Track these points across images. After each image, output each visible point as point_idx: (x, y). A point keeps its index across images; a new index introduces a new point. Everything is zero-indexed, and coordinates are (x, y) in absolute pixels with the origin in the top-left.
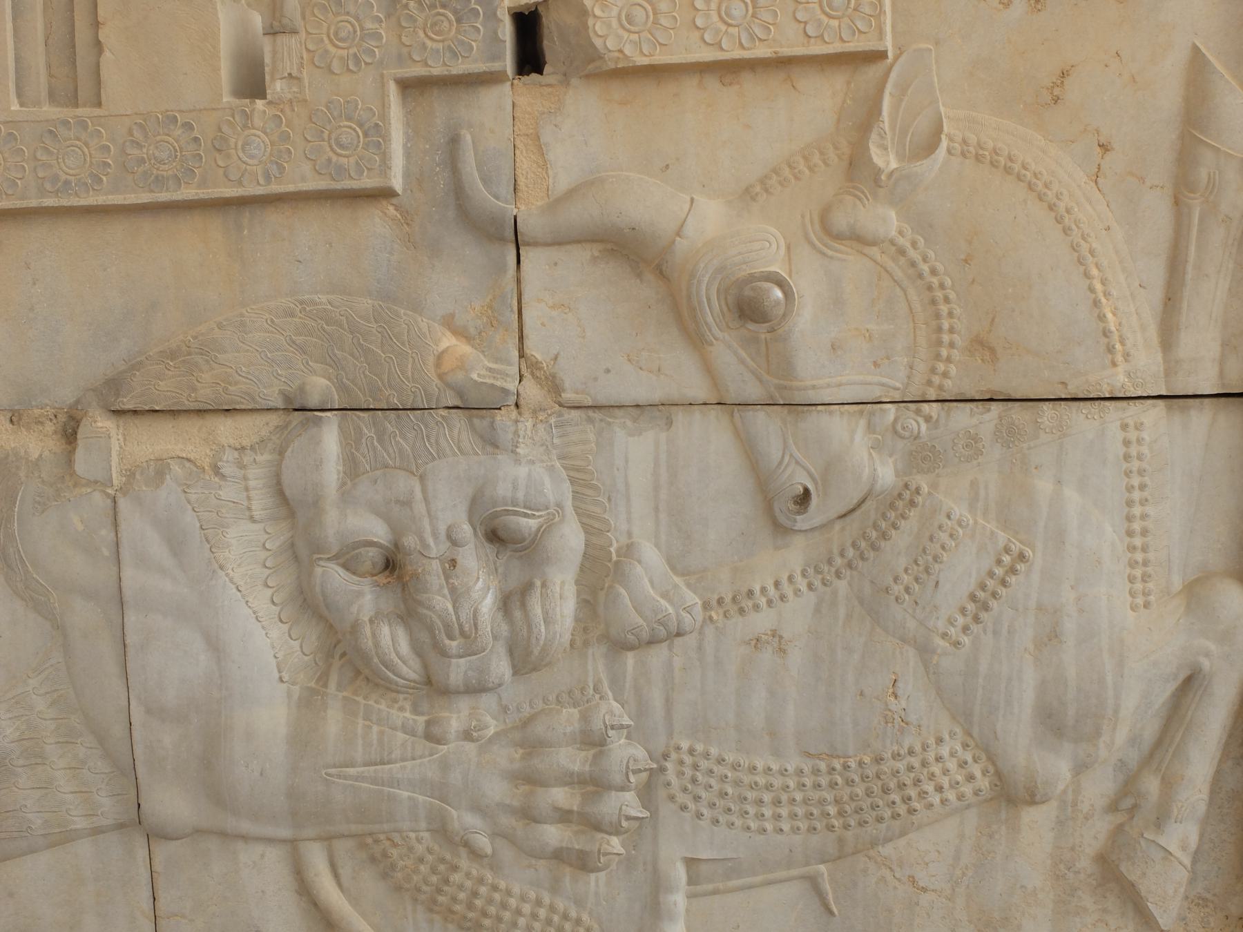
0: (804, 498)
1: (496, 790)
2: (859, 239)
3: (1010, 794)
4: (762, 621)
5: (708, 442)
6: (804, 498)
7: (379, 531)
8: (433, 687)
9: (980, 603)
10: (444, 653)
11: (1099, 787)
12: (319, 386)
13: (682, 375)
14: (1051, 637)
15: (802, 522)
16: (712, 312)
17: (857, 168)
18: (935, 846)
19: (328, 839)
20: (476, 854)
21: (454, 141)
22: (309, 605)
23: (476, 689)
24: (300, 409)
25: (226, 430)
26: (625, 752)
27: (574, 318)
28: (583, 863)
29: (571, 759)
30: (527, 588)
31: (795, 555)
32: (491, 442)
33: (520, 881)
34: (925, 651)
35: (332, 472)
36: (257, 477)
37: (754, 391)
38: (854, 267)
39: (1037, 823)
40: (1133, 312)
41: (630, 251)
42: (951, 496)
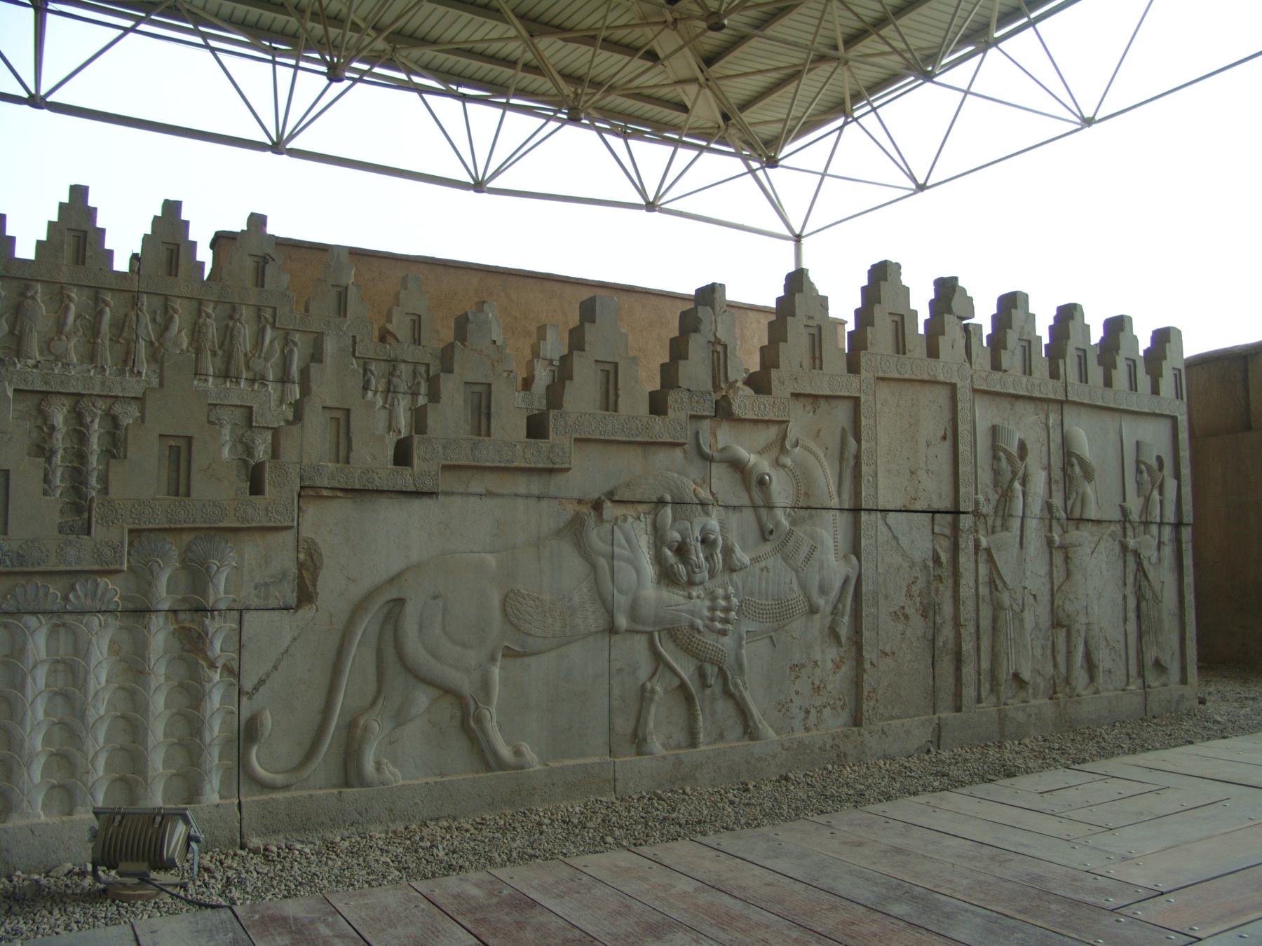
0: (771, 532)
1: (706, 613)
2: (784, 466)
3: (813, 610)
4: (763, 564)
5: (748, 515)
6: (771, 532)
7: (677, 536)
8: (691, 583)
9: (808, 559)
10: (694, 572)
11: (829, 609)
12: (668, 498)
13: (745, 500)
14: (821, 568)
15: (771, 538)
16: (754, 483)
17: (783, 449)
18: (796, 625)
19: (659, 632)
20: (699, 632)
21: (697, 433)
22: (659, 559)
23: (701, 583)
24: (661, 502)
25: (641, 508)
26: (735, 600)
27: (722, 482)
28: (723, 633)
29: (723, 603)
30: (712, 555)
31: (768, 547)
32: (707, 514)
33: (709, 639)
34: (797, 572)
35: (669, 521)
36: (649, 521)
37: (761, 503)
38: (782, 472)
39: (817, 617)
40: (833, 489)
41: (737, 466)
42: (799, 532)
